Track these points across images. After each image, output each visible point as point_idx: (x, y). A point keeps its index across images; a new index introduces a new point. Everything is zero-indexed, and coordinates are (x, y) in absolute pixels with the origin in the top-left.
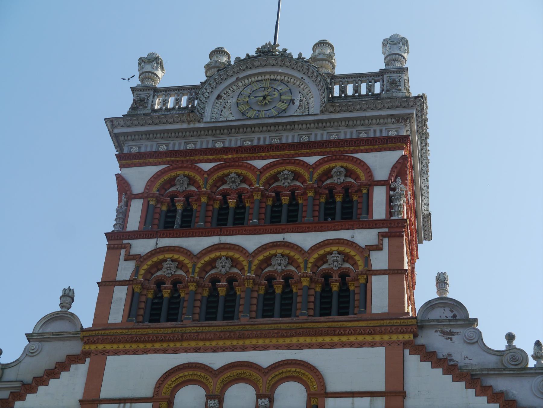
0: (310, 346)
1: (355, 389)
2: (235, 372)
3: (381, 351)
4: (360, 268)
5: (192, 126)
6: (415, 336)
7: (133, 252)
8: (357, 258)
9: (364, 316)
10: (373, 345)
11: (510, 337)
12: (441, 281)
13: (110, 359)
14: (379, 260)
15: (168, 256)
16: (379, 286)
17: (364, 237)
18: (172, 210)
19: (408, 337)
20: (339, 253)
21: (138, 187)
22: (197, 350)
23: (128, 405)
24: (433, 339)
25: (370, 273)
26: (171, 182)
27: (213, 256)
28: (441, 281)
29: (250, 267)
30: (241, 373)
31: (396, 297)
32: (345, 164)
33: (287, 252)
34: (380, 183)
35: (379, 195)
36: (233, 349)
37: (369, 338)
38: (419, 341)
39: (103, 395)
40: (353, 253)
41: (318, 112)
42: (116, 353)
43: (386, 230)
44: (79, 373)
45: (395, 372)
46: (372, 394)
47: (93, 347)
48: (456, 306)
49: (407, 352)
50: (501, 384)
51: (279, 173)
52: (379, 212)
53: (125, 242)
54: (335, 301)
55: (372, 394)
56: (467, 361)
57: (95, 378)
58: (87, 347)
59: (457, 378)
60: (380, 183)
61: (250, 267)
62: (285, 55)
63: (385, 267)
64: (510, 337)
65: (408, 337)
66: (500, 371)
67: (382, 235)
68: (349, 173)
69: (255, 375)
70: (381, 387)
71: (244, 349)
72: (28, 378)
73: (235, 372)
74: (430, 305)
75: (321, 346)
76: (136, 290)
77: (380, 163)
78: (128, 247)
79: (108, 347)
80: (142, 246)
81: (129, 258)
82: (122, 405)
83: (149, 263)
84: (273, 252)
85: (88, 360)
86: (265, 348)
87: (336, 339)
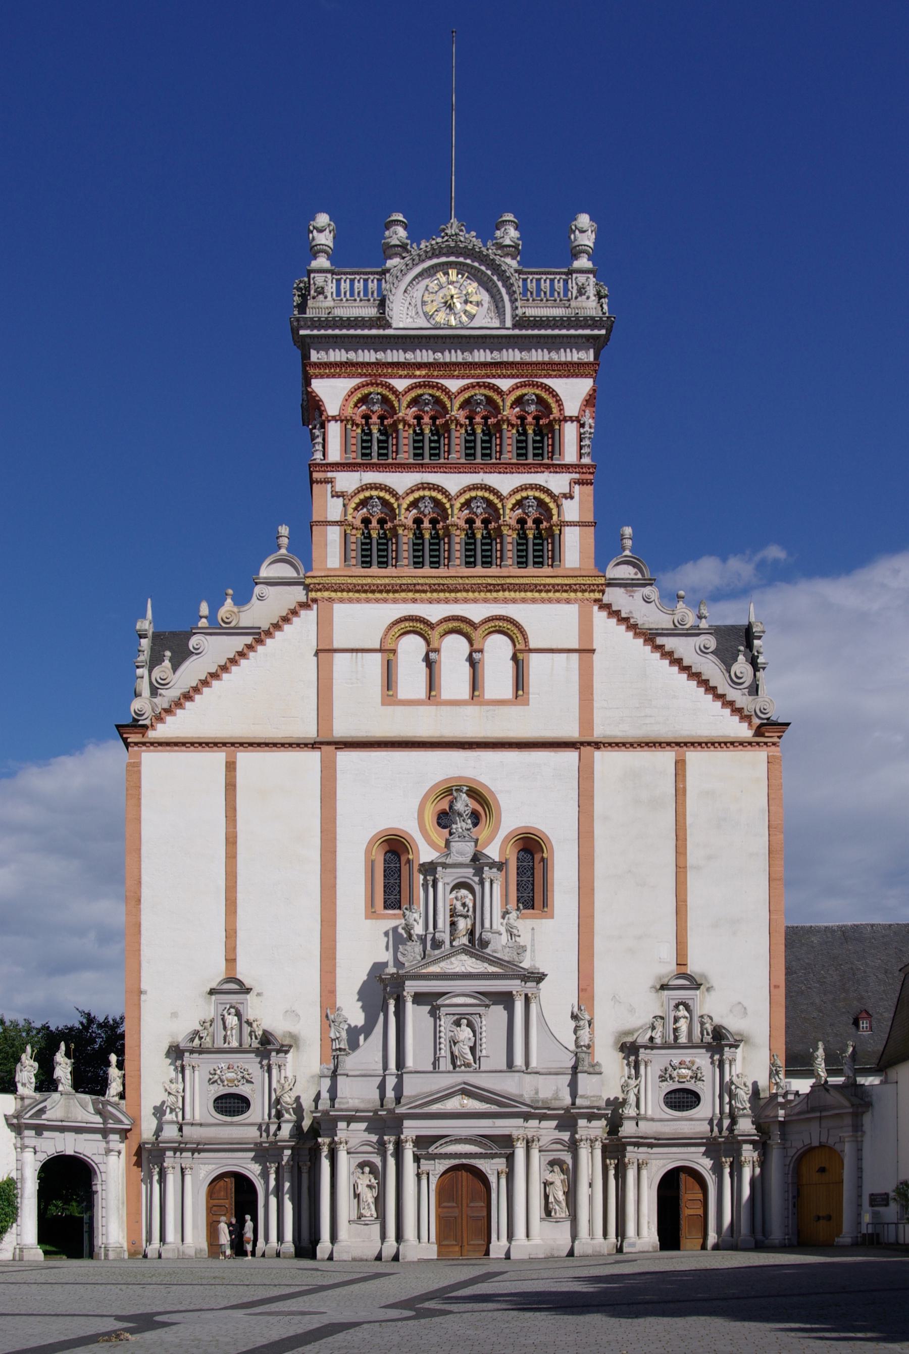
0: (514, 601)
1: (554, 647)
2: (451, 625)
3: (574, 609)
4: (555, 518)
6: (603, 592)
7: (339, 488)
8: (552, 505)
9: (559, 571)
10: (568, 601)
13: (337, 607)
17: (557, 483)
19: (597, 595)
20: (535, 498)
21: (332, 408)
22: (414, 601)
23: (359, 654)
25: (563, 524)
26: (364, 400)
27: (416, 495)
29: (452, 511)
32: (537, 392)
33: (487, 495)
36: (447, 601)
38: (606, 599)
39: (336, 645)
40: (547, 500)
41: (509, 323)
42: (341, 601)
43: (577, 476)
44: (308, 619)
49: (596, 608)
51: (472, 396)
52: (570, 455)
53: (330, 475)
56: (645, 618)
57: (324, 626)
58: (313, 595)
59: (637, 635)
60: (571, 419)
61: (452, 511)
65: (597, 595)
66: (672, 633)
68: (540, 401)
69: (468, 629)
70: (576, 646)
71: (456, 601)
72: (265, 626)
73: (451, 625)
75: (524, 601)
76: (348, 532)
78: (330, 481)
79: (333, 595)
80: (347, 481)
81: (336, 495)
82: (354, 654)
83: (357, 500)
84: (473, 494)
85: (315, 606)
86: (475, 601)
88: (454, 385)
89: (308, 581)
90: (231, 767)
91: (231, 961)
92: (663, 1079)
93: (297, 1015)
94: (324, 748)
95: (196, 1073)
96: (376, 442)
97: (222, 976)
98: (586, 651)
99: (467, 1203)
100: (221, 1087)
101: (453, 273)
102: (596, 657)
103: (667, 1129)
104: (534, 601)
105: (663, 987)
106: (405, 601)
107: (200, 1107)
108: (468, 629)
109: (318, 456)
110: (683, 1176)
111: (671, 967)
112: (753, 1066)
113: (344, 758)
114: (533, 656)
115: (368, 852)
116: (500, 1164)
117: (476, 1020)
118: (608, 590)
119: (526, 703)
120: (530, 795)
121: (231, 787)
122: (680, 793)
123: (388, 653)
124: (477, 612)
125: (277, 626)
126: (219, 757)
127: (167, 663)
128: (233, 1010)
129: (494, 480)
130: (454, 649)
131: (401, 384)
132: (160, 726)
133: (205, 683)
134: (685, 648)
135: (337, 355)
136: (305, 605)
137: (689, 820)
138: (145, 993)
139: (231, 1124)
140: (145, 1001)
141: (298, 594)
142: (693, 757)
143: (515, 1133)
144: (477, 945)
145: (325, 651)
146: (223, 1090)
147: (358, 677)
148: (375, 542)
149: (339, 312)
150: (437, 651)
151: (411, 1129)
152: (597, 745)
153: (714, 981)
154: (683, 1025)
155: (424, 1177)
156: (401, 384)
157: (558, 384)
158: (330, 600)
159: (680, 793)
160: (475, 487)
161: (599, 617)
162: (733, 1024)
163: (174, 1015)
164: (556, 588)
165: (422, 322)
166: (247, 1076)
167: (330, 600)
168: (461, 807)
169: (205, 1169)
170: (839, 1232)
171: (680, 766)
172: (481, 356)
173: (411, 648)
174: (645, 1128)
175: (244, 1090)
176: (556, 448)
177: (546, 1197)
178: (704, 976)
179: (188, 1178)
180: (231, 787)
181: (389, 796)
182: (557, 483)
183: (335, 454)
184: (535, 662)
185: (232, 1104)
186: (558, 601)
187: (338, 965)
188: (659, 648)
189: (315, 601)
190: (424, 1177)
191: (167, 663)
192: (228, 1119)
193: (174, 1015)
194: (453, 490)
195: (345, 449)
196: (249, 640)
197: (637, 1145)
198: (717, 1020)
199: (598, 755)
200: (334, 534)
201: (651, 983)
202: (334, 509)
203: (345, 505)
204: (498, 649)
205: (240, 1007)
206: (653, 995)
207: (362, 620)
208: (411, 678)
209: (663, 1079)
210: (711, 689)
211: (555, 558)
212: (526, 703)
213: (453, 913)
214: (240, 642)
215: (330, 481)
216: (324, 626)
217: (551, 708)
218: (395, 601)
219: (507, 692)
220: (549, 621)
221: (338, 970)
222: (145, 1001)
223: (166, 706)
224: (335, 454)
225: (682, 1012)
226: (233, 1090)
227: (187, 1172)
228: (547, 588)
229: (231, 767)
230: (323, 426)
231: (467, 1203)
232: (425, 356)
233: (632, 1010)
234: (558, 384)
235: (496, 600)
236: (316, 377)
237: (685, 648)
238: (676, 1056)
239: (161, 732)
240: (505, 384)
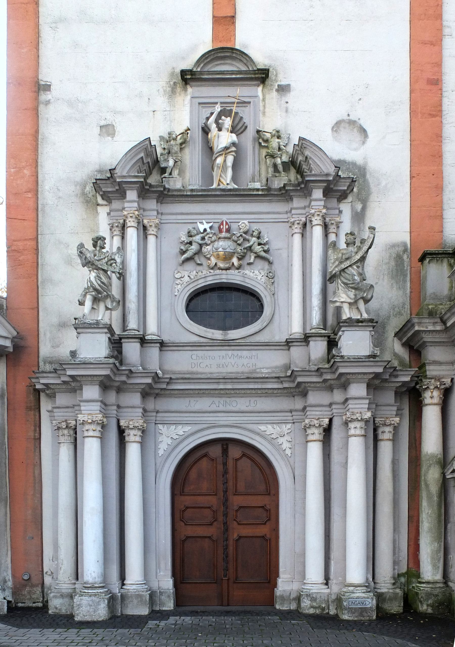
93: (363, 131)
95: (151, 240)
97: (206, 44)
100: (205, 272)
107: (161, 306)
128: (227, 122)
138: (47, 88)
139: (227, 344)
140: (48, 103)
146: (206, 277)
166: (258, 249)
169: (175, 438)
175: (253, 276)
185: (224, 304)
187: (446, 31)
192: (218, 334)
205: (246, 114)
221: (447, 43)
222: (48, 103)
226: (234, 277)
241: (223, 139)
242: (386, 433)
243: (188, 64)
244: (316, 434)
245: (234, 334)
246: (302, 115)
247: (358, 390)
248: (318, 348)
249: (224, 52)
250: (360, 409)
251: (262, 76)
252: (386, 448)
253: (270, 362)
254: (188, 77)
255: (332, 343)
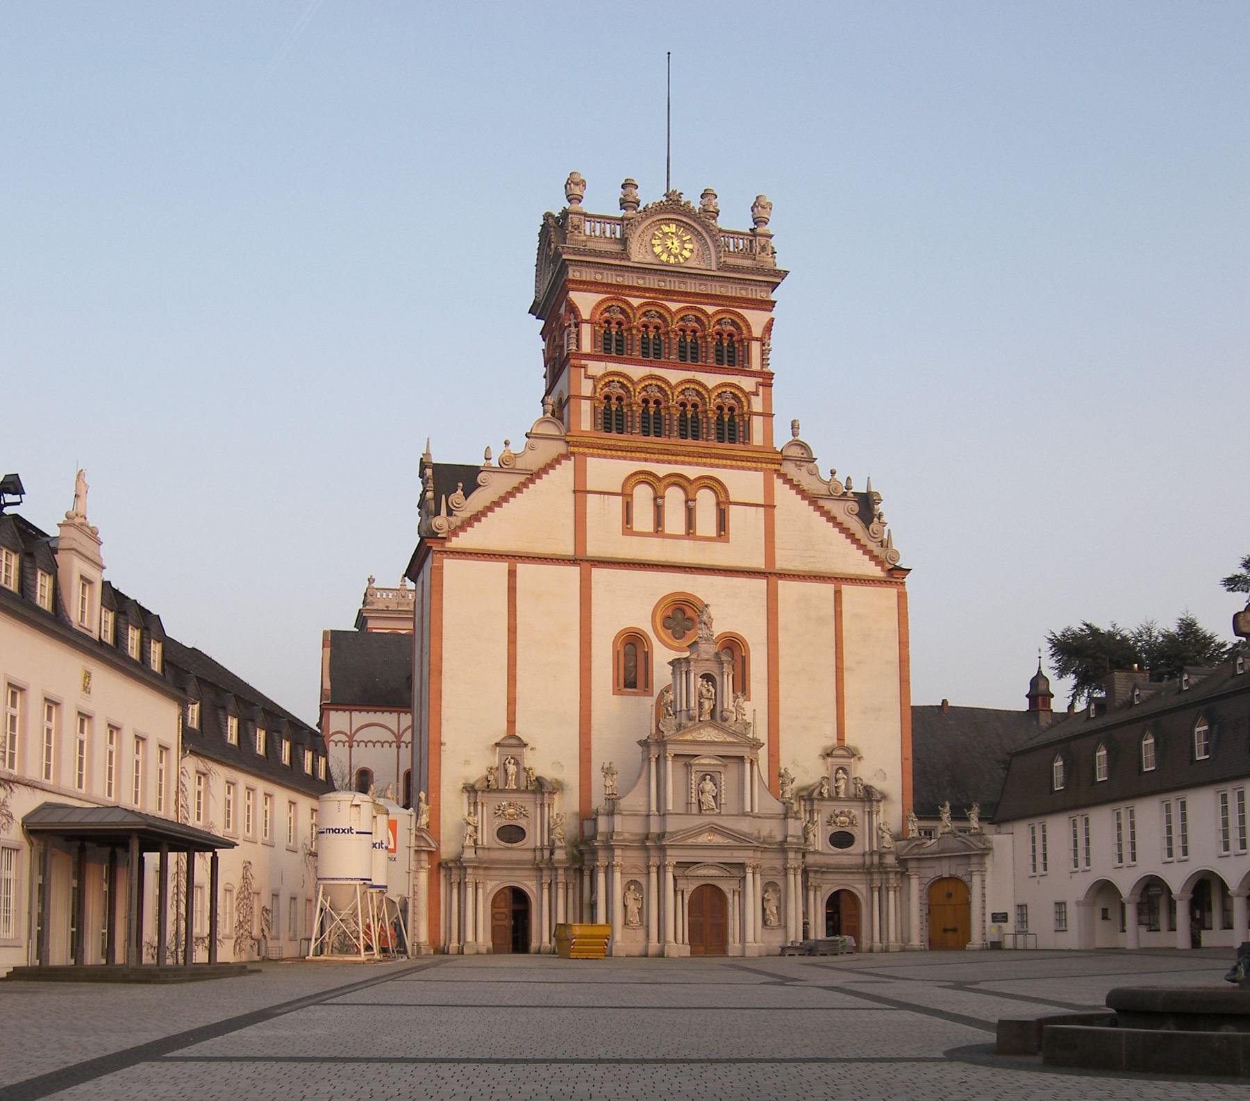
0: (718, 466)
2: (673, 480)
5: (623, 263)
9: (749, 447)
10: (756, 470)
11: (833, 473)
12: (794, 426)
14: (757, 404)
15: (616, 379)
16: (757, 424)
17: (748, 384)
18: (607, 334)
19: (777, 467)
21: (585, 315)
22: (646, 460)
24: (789, 468)
26: (607, 310)
28: (794, 426)
30: (678, 481)
31: (768, 433)
34: (757, 339)
35: (756, 348)
37: (754, 465)
38: (783, 470)
42: (592, 455)
44: (567, 467)
45: (769, 490)
46: (757, 505)
47: (575, 449)
48: (803, 446)
50: (828, 505)
52: (756, 365)
53: (583, 362)
54: (728, 427)
55: (757, 505)
57: (580, 473)
58: (572, 449)
59: (804, 498)
60: (757, 339)
62: (689, 212)
63: (761, 411)
64: (833, 473)
66: (829, 497)
67: (759, 384)
68: (734, 323)
69: (685, 483)
71: (676, 463)
72: (535, 469)
73: (673, 480)
74: (790, 444)
75: (725, 467)
77: (755, 319)
78: (585, 367)
79: (586, 450)
87: (734, 463)
88: (674, 306)
89: (568, 439)
90: (512, 574)
91: (511, 722)
92: (829, 824)
94: (583, 564)
96: (613, 344)
98: (769, 507)
99: (709, 917)
101: (673, 228)
102: (776, 511)
103: (832, 861)
104: (732, 467)
105: (828, 755)
106: (639, 459)
108: (685, 483)
109: (574, 347)
110: (843, 896)
111: (833, 741)
112: (892, 814)
113: (598, 574)
114: (732, 507)
115: (614, 644)
116: (734, 884)
117: (716, 776)
118: (785, 463)
119: (727, 541)
120: (732, 609)
121: (512, 589)
122: (838, 615)
123: (626, 495)
124: (692, 472)
125: (545, 470)
126: (503, 567)
127: (459, 491)
129: (702, 377)
130: (674, 496)
131: (636, 302)
132: (454, 539)
133: (490, 509)
134: (837, 509)
135: (588, 275)
136: (566, 457)
137: (845, 634)
141: (560, 448)
142: (847, 589)
143: (747, 861)
144: (717, 717)
145: (580, 492)
147: (604, 513)
148: (612, 417)
149: (590, 245)
150: (663, 497)
151: (673, 857)
152: (783, 575)
153: (863, 753)
154: (842, 784)
155: (679, 894)
156: (636, 302)
157: (748, 314)
158: (585, 454)
159: (838, 615)
160: (689, 381)
161: (778, 482)
162: (878, 785)
163: (467, 762)
164: (748, 459)
165: (650, 259)
167: (585, 454)
168: (681, 616)
169: (492, 885)
170: (968, 939)
171: (838, 594)
172: (693, 286)
173: (643, 495)
174: (819, 859)
175: (522, 823)
176: (747, 358)
177: (764, 910)
178: (855, 748)
179: (480, 891)
180: (512, 589)
181: (629, 603)
182: (748, 384)
183: (586, 347)
184: (734, 512)
185: (511, 834)
186: (749, 469)
188: (819, 508)
189: (573, 454)
190: (679, 894)
191: (459, 491)
192: (509, 845)
193: (467, 762)
194: (673, 382)
195: (594, 344)
196: (522, 478)
197: (816, 872)
198: (866, 782)
199: (781, 583)
200: (586, 406)
201: (820, 751)
202: (587, 388)
203: (595, 386)
204: (706, 501)
205: (518, 758)
206: (821, 761)
207: (607, 471)
208: (643, 519)
209: (829, 824)
210: (855, 541)
211: (747, 436)
212: (727, 541)
213: (701, 695)
214: (516, 480)
215: (585, 367)
216: (580, 473)
217: (744, 547)
218: (632, 459)
219: (712, 532)
220: (744, 483)
223: (459, 524)
224: (586, 347)
225: (841, 775)
227: (480, 886)
228: (741, 459)
229: (512, 574)
230: (577, 325)
231: (709, 917)
232: (652, 282)
233: (807, 773)
234: (748, 314)
235: (705, 465)
236: (573, 290)
237: (837, 509)
238: (837, 807)
239: (456, 543)
240: (710, 310)
241: (512, 769)
242: (570, 886)
243: (497, 740)
244: (546, 886)
245: (515, 845)
246: (540, 763)
247: (561, 872)
248: (547, 854)
249: (511, 734)
250: (561, 877)
251: (526, 745)
252: (570, 891)
253: (528, 856)
254: (497, 744)
255: (552, 853)
